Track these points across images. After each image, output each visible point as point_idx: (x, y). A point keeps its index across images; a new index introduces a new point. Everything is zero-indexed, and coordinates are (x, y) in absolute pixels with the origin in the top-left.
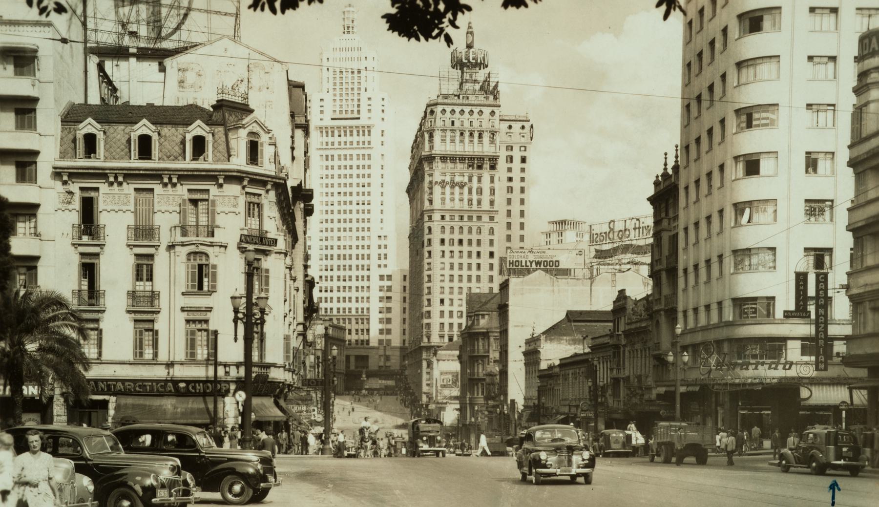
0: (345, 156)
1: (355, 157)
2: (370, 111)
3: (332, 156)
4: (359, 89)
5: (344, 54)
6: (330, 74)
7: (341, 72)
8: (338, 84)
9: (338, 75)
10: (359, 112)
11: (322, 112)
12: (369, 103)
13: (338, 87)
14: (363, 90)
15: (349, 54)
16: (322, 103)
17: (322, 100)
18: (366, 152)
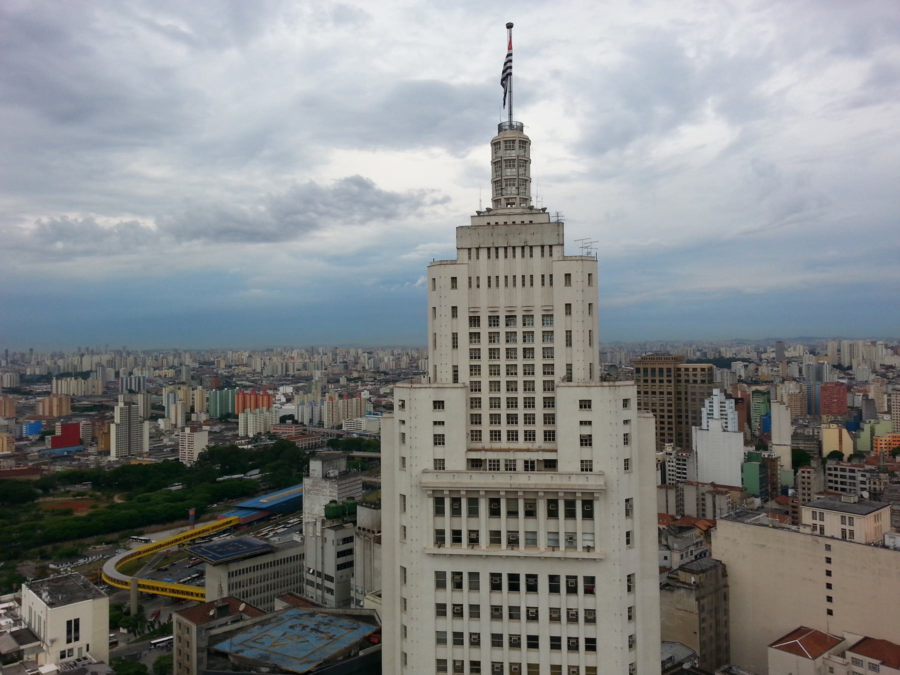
0: (514, 579)
1: (543, 584)
2: (586, 441)
3: (474, 576)
4: (548, 369)
5: (502, 266)
6: (463, 328)
7: (494, 320)
8: (485, 354)
9: (484, 329)
10: (550, 436)
11: (439, 440)
12: (585, 415)
13: (485, 362)
14: (560, 372)
15: (518, 265)
16: (439, 416)
17: (439, 405)
18: (581, 572)
